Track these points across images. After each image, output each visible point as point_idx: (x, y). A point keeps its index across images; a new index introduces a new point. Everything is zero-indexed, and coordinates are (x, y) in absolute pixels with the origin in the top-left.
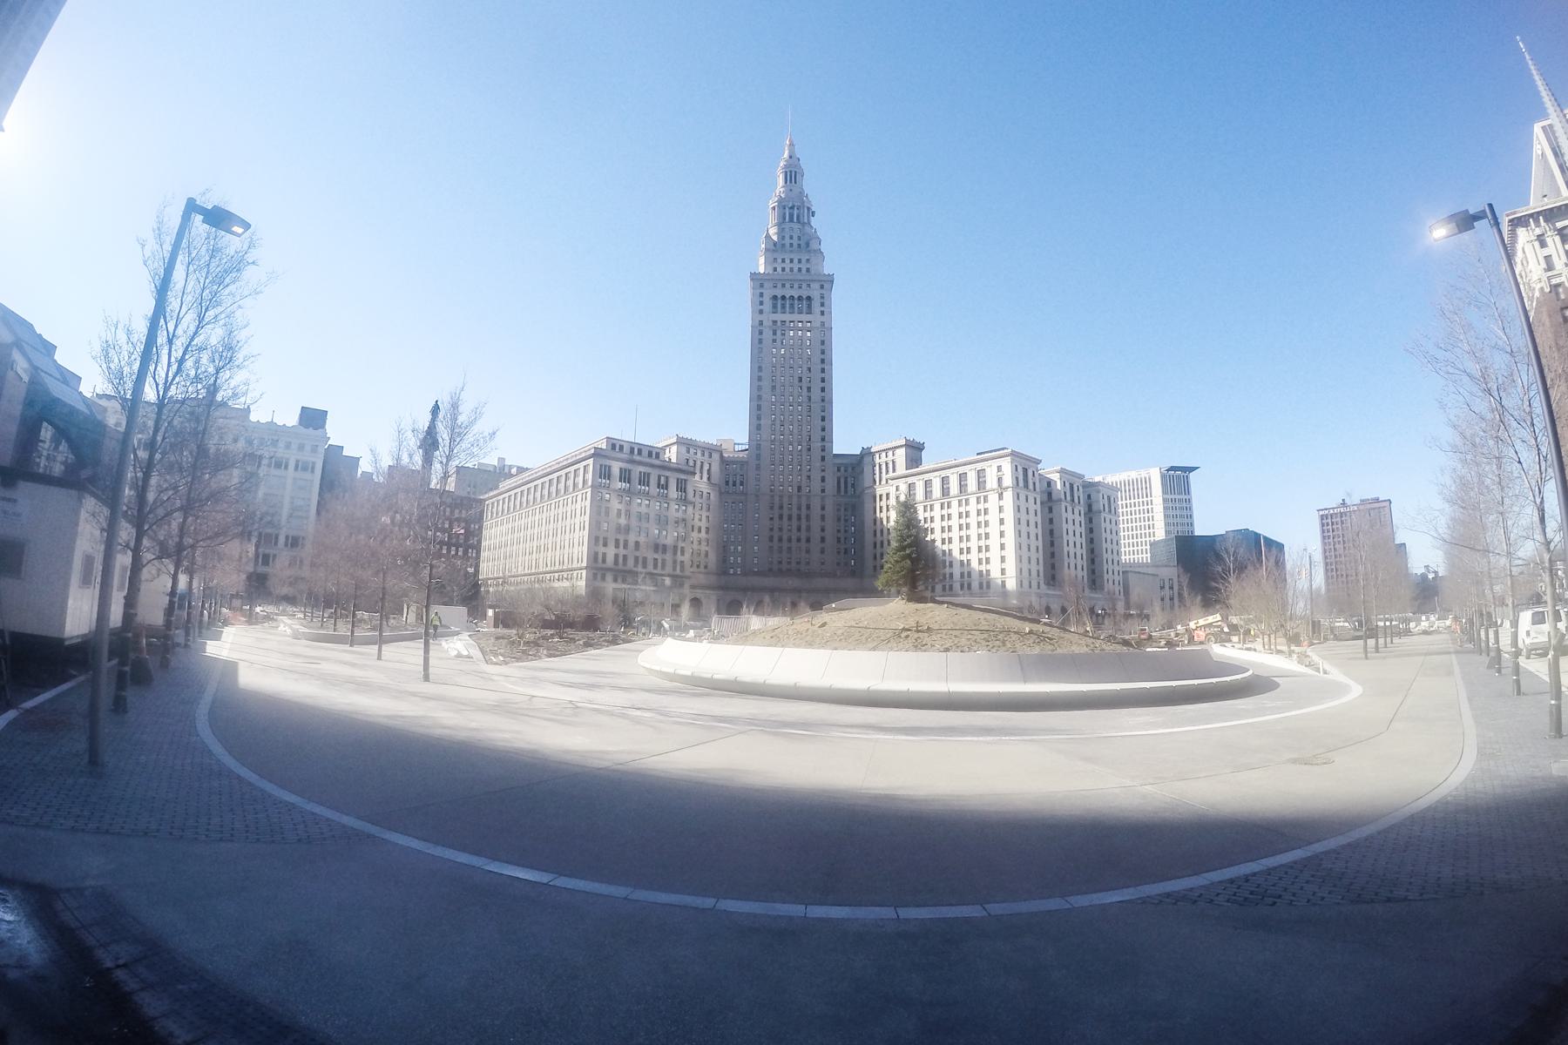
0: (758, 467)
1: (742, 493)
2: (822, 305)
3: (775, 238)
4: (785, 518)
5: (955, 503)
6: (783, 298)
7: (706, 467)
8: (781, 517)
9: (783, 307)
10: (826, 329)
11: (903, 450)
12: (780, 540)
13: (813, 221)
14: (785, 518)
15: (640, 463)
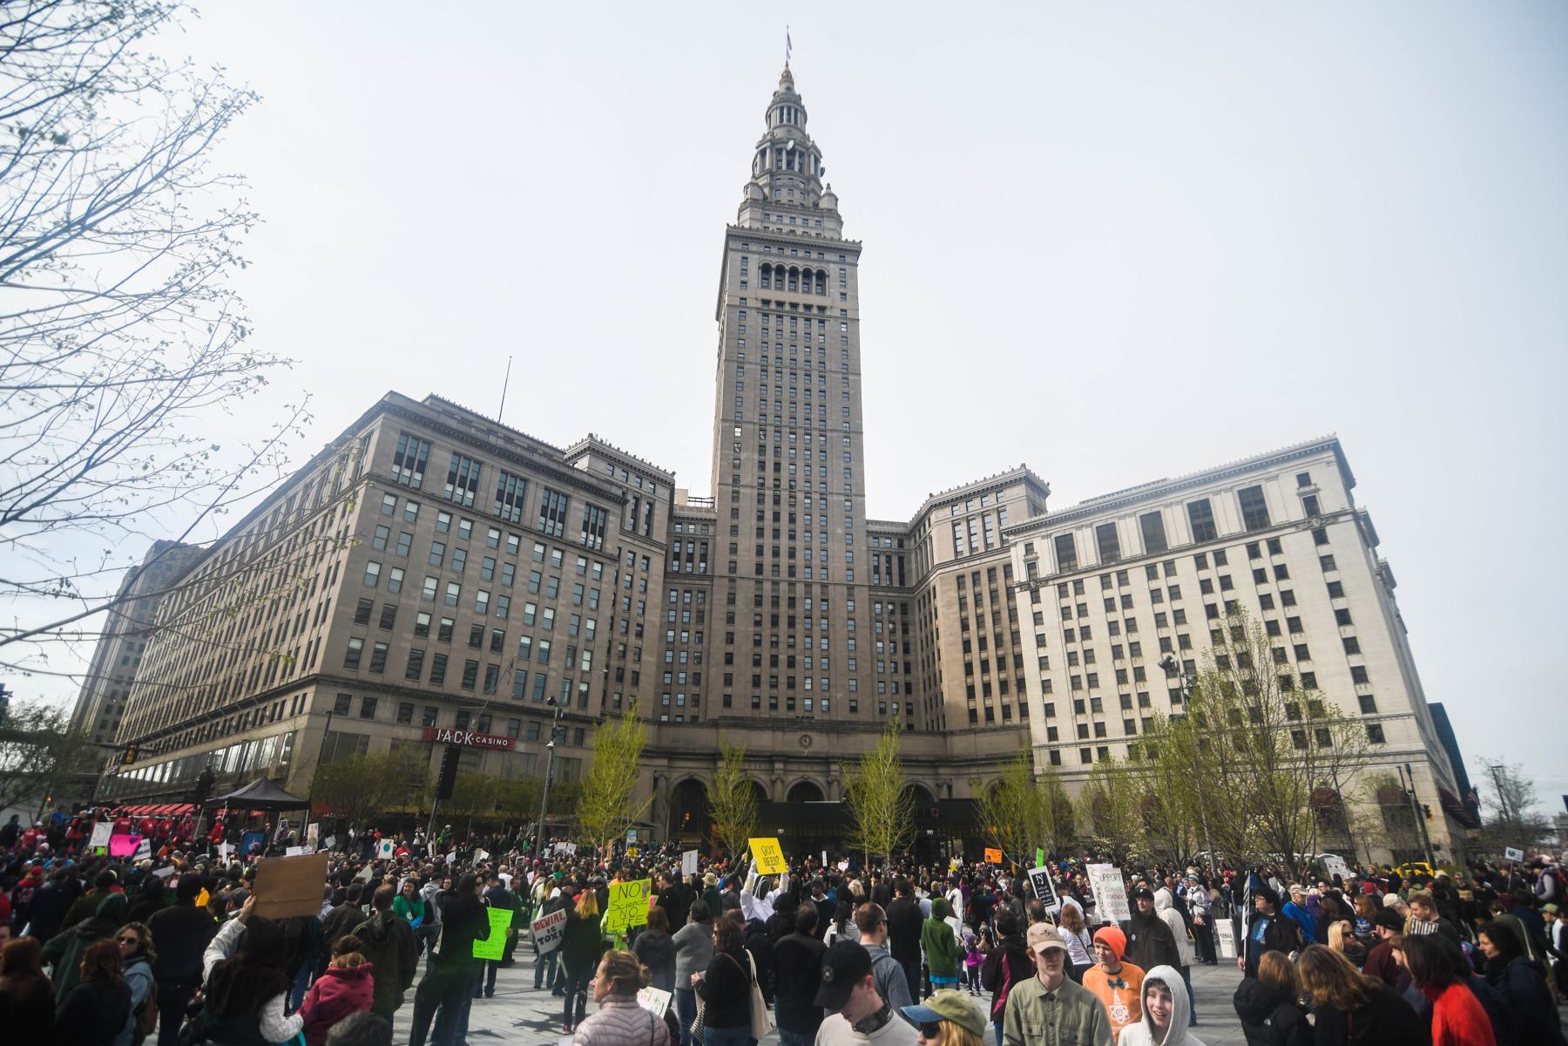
0: (734, 530)
1: (703, 576)
2: (843, 281)
3: (766, 190)
4: (783, 622)
5: (1185, 564)
6: (780, 270)
7: (644, 509)
8: (775, 621)
9: (780, 280)
10: (850, 319)
11: (1020, 491)
12: (774, 662)
13: (823, 181)
14: (783, 622)
15: (502, 454)
